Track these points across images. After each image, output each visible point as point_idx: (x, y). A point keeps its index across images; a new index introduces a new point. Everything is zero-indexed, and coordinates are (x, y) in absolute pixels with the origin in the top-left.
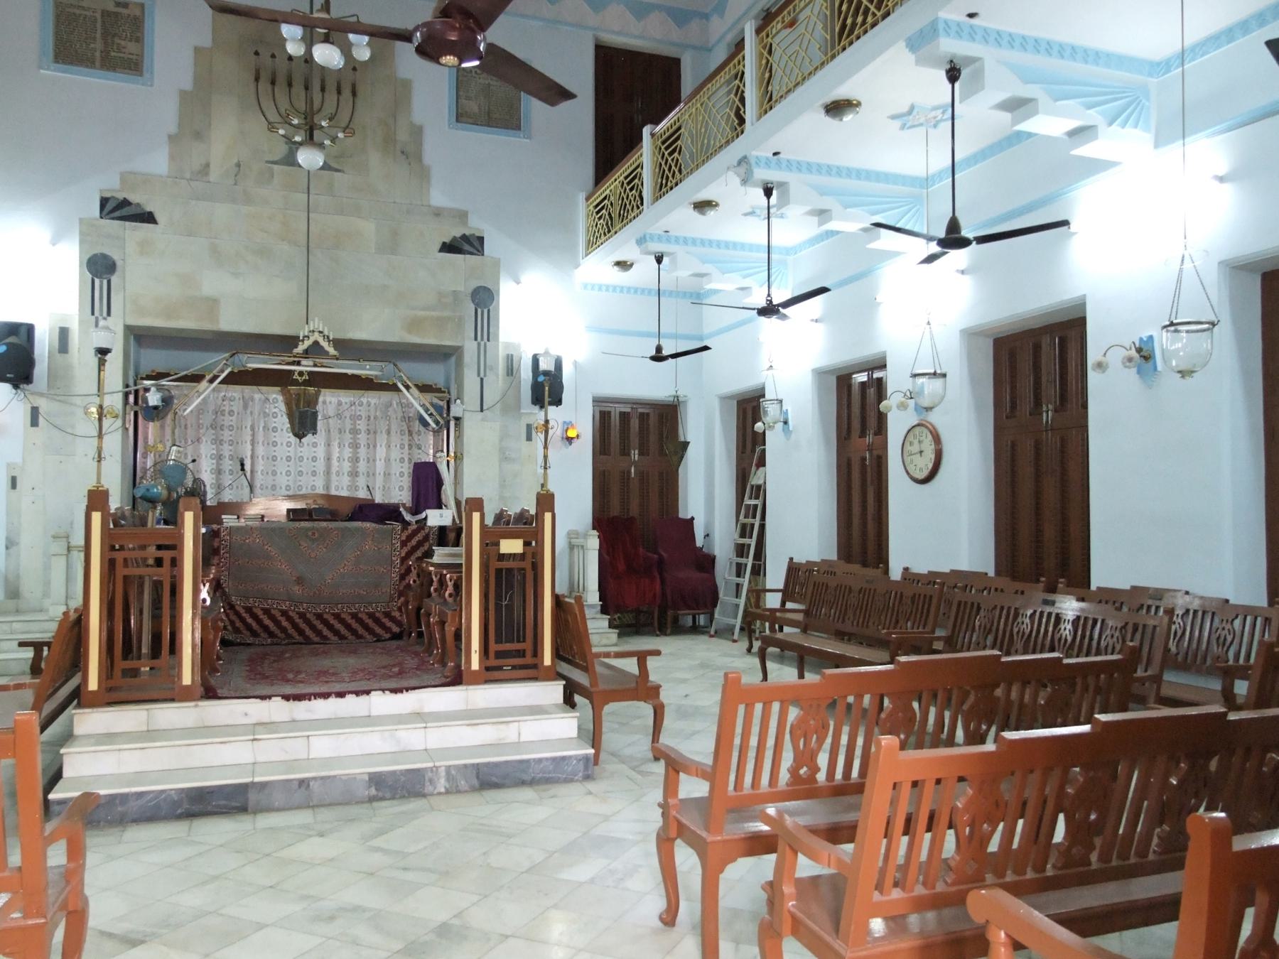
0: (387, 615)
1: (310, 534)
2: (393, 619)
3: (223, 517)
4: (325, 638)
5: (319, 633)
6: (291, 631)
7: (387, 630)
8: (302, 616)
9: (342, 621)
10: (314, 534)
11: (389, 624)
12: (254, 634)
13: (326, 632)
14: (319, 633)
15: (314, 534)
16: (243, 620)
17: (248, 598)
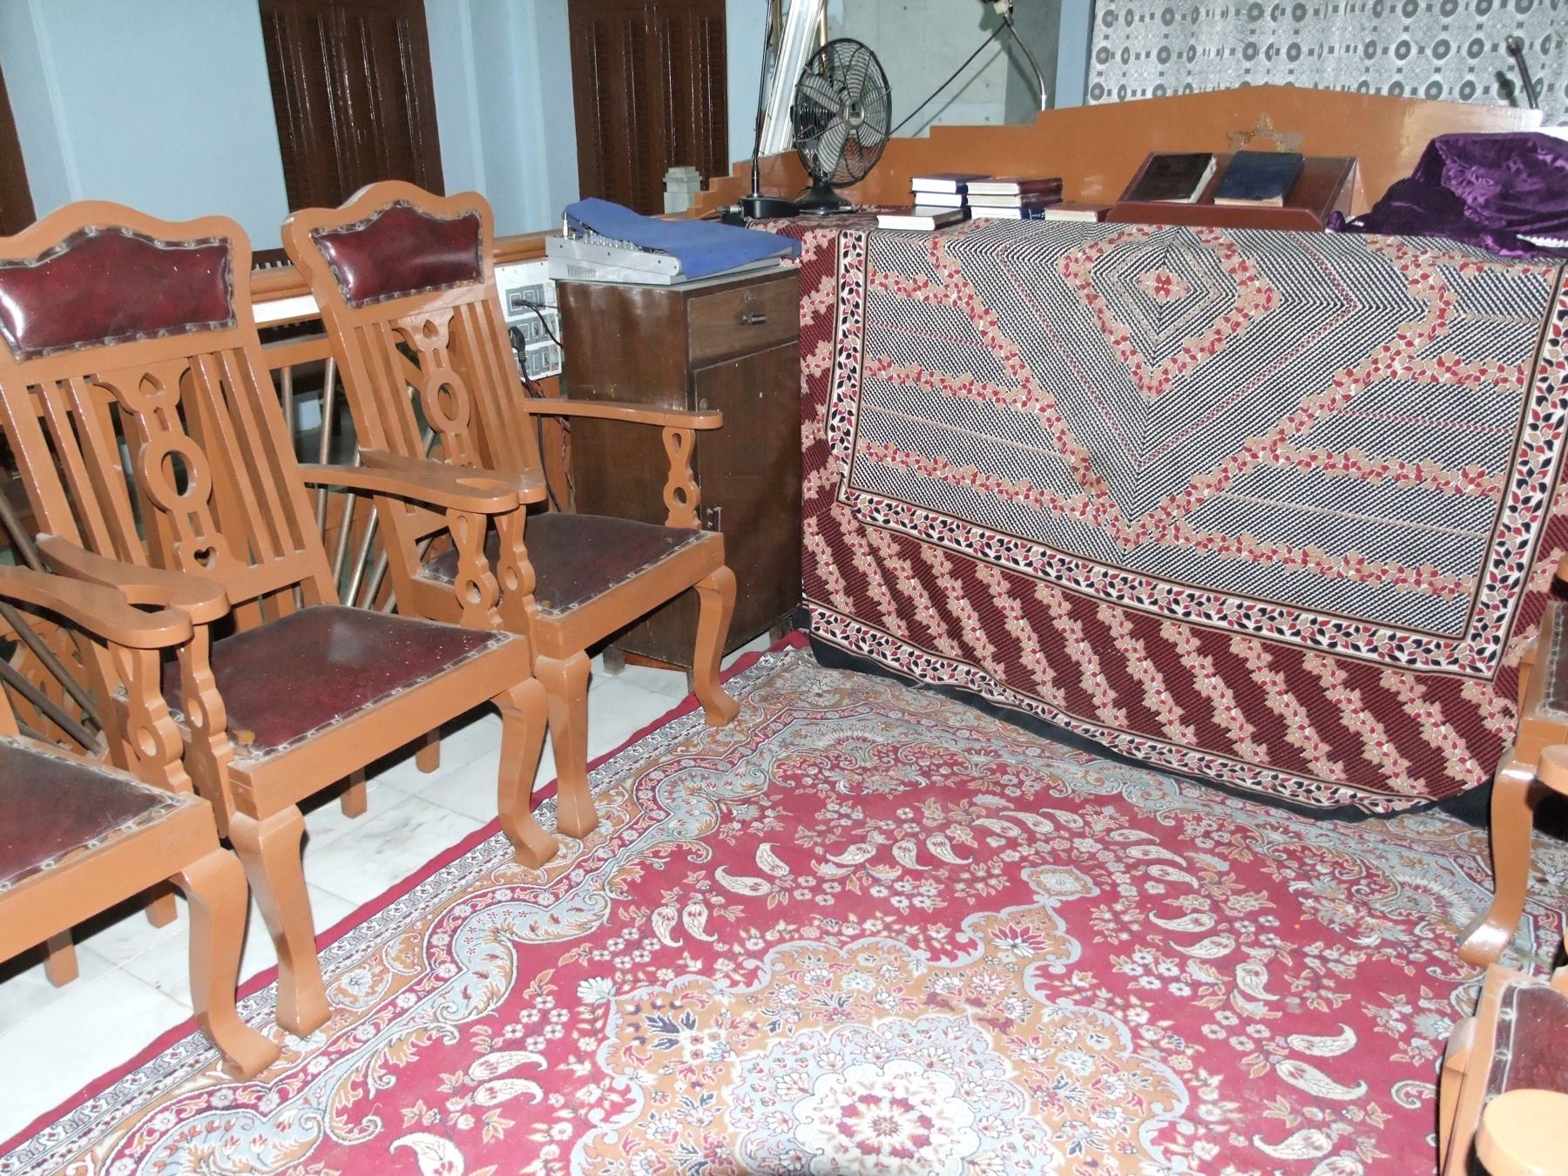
0: (1442, 689)
1: (1149, 281)
2: (1465, 719)
3: (918, 184)
4: (1144, 722)
5: (1129, 694)
6: (1032, 657)
7: (1427, 762)
8: (1083, 609)
9: (1233, 671)
10: (1164, 285)
11: (1437, 732)
12: (919, 636)
13: (1157, 696)
14: (1129, 694)
15: (1164, 285)
16: (889, 578)
17: (911, 508)
